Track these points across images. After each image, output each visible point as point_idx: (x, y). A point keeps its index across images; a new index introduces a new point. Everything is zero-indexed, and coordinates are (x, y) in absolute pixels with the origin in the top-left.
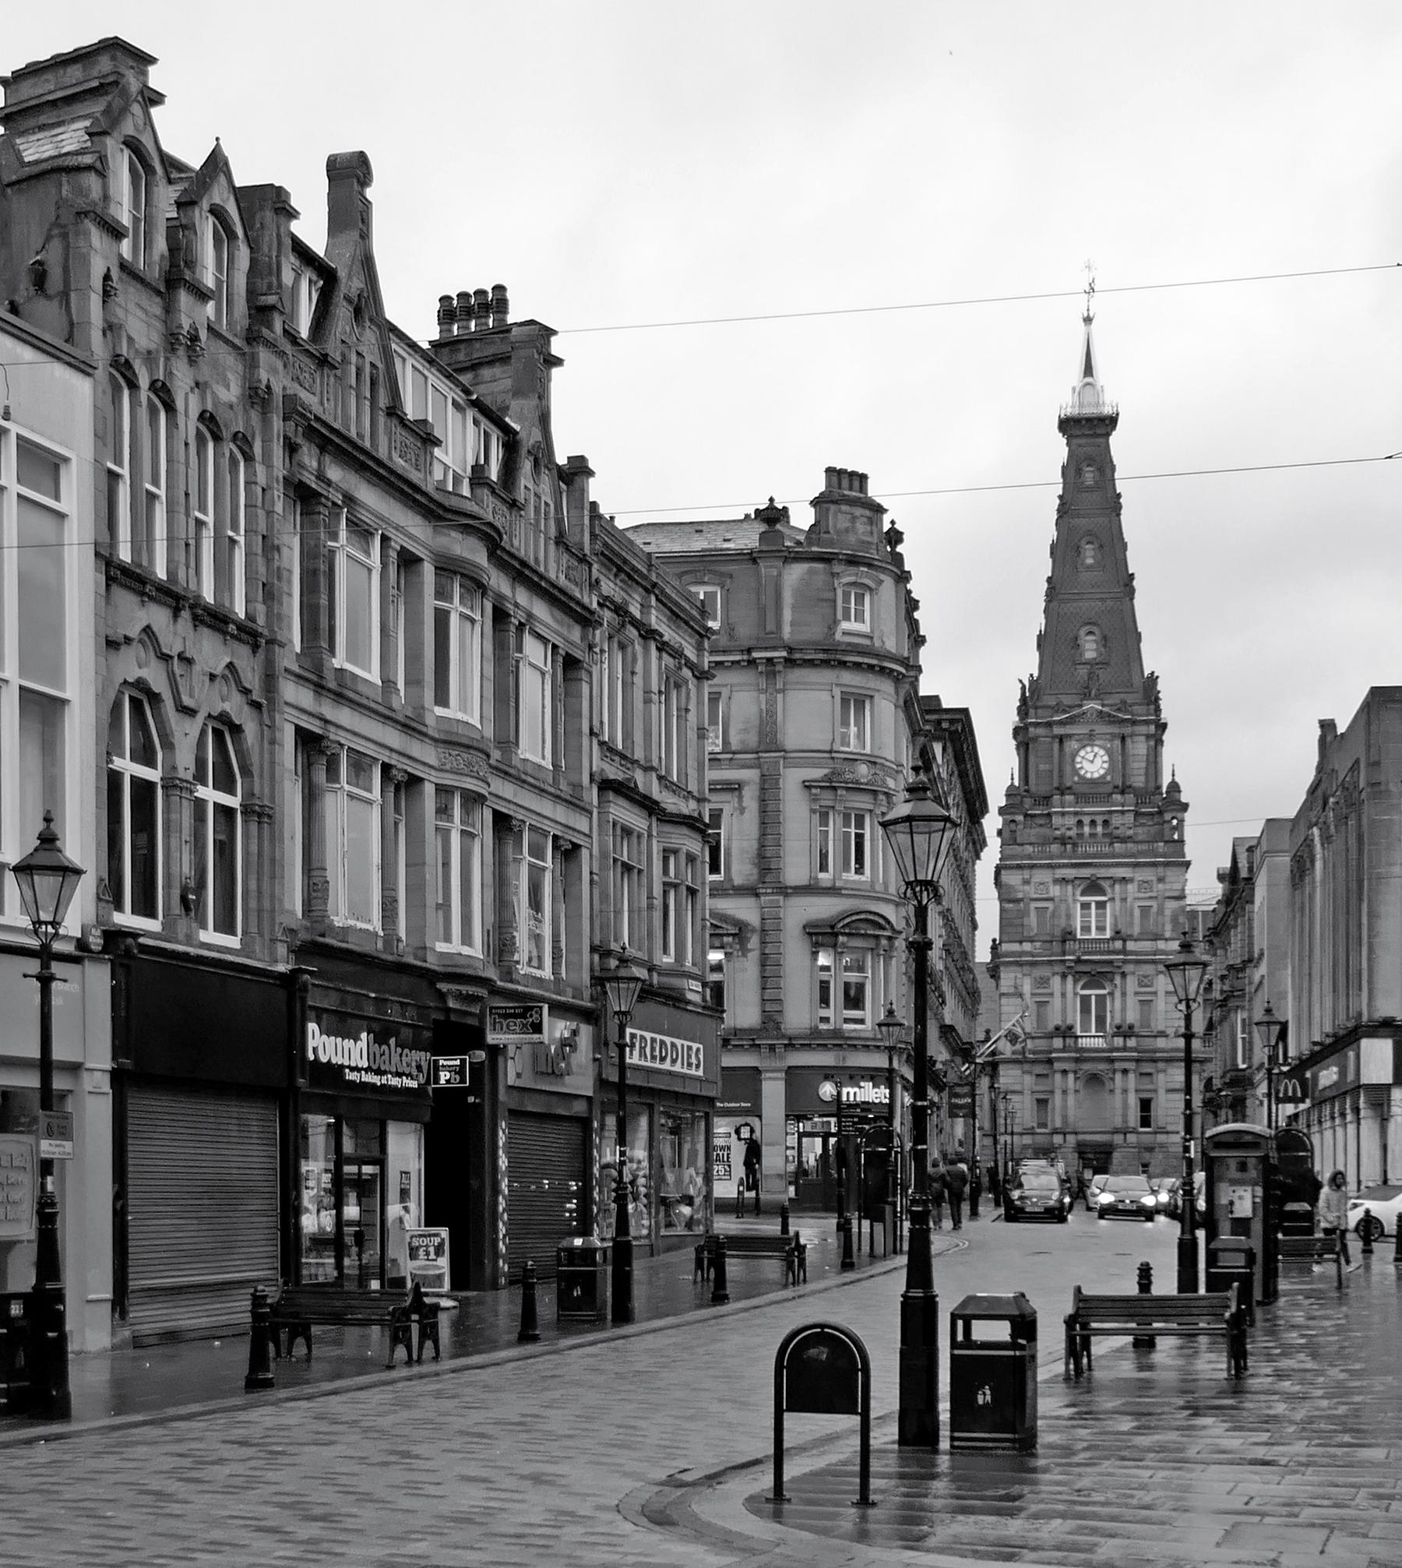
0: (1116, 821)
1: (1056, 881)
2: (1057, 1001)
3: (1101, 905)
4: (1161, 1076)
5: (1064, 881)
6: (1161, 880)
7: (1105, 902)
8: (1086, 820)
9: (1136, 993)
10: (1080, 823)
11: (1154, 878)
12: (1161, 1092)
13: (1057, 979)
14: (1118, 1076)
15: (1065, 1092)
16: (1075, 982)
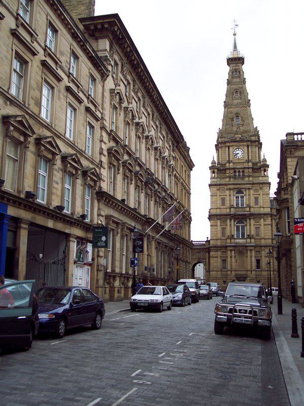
0: (246, 171)
1: (227, 189)
2: (228, 227)
3: (242, 197)
5: (230, 189)
6: (261, 189)
8: (237, 170)
9: (254, 225)
10: (235, 172)
13: (228, 221)
14: (249, 252)
15: (231, 257)
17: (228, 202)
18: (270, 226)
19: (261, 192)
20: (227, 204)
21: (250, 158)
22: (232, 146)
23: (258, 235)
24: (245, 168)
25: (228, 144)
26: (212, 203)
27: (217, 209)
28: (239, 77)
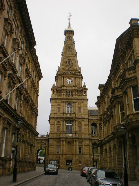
3: (71, 108)
4: (83, 142)
5: (63, 102)
6: (83, 102)
7: (72, 107)
8: (68, 91)
10: (67, 92)
11: (81, 102)
12: (83, 146)
13: (62, 121)
14: (74, 142)
16: (65, 122)
17: (62, 110)
18: (88, 126)
19: (82, 104)
20: (62, 111)
21: (76, 85)
22: (65, 77)
23: (80, 131)
24: (73, 90)
25: (63, 76)
26: (52, 110)
27: (55, 114)
28: (71, 41)
